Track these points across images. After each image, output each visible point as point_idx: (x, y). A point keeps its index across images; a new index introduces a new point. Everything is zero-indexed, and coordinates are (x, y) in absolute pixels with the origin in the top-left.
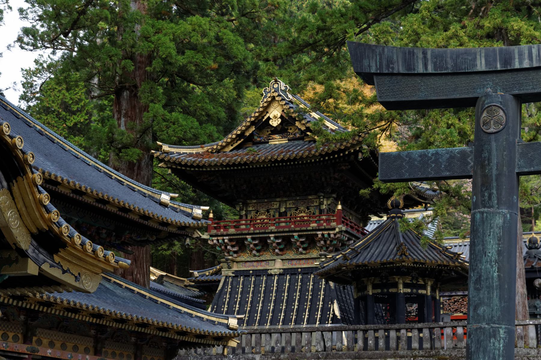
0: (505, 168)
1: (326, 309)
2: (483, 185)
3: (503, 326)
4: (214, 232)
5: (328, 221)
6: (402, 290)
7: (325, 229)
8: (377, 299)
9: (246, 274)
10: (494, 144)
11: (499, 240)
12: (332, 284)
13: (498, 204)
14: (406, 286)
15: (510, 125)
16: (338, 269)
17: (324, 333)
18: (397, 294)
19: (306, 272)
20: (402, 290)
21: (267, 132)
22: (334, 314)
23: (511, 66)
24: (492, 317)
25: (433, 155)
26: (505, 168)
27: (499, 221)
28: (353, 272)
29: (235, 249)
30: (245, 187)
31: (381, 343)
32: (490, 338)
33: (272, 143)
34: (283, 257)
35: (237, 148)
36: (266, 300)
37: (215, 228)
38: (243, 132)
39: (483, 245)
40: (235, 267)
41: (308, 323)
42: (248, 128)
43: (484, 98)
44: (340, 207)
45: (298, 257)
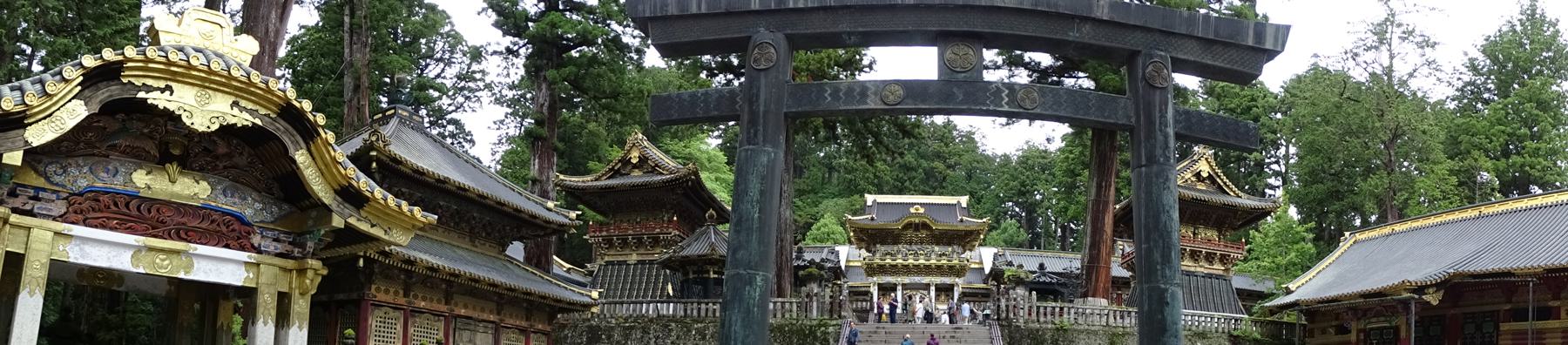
0: (772, 106)
1: (664, 289)
2: (749, 122)
3: (761, 273)
4: (592, 234)
5: (668, 228)
6: (712, 275)
7: (665, 234)
8: (695, 282)
9: (612, 263)
10: (763, 81)
11: (762, 179)
12: (668, 271)
13: (763, 141)
14: (714, 273)
15: (781, 63)
16: (669, 259)
17: (659, 305)
18: (709, 278)
19: (651, 262)
20: (712, 275)
21: (630, 167)
22: (668, 293)
23: (785, 5)
24: (749, 262)
25: (702, 94)
26: (772, 106)
27: (765, 159)
28: (681, 262)
29: (607, 246)
30: (613, 204)
31: (695, 313)
32: (746, 285)
33: (632, 174)
34: (639, 252)
35: (609, 178)
36: (625, 282)
37: (593, 232)
38: (613, 167)
39: (746, 183)
40: (606, 259)
41: (651, 297)
42: (617, 164)
43: (755, 37)
44: (675, 218)
45: (646, 252)
